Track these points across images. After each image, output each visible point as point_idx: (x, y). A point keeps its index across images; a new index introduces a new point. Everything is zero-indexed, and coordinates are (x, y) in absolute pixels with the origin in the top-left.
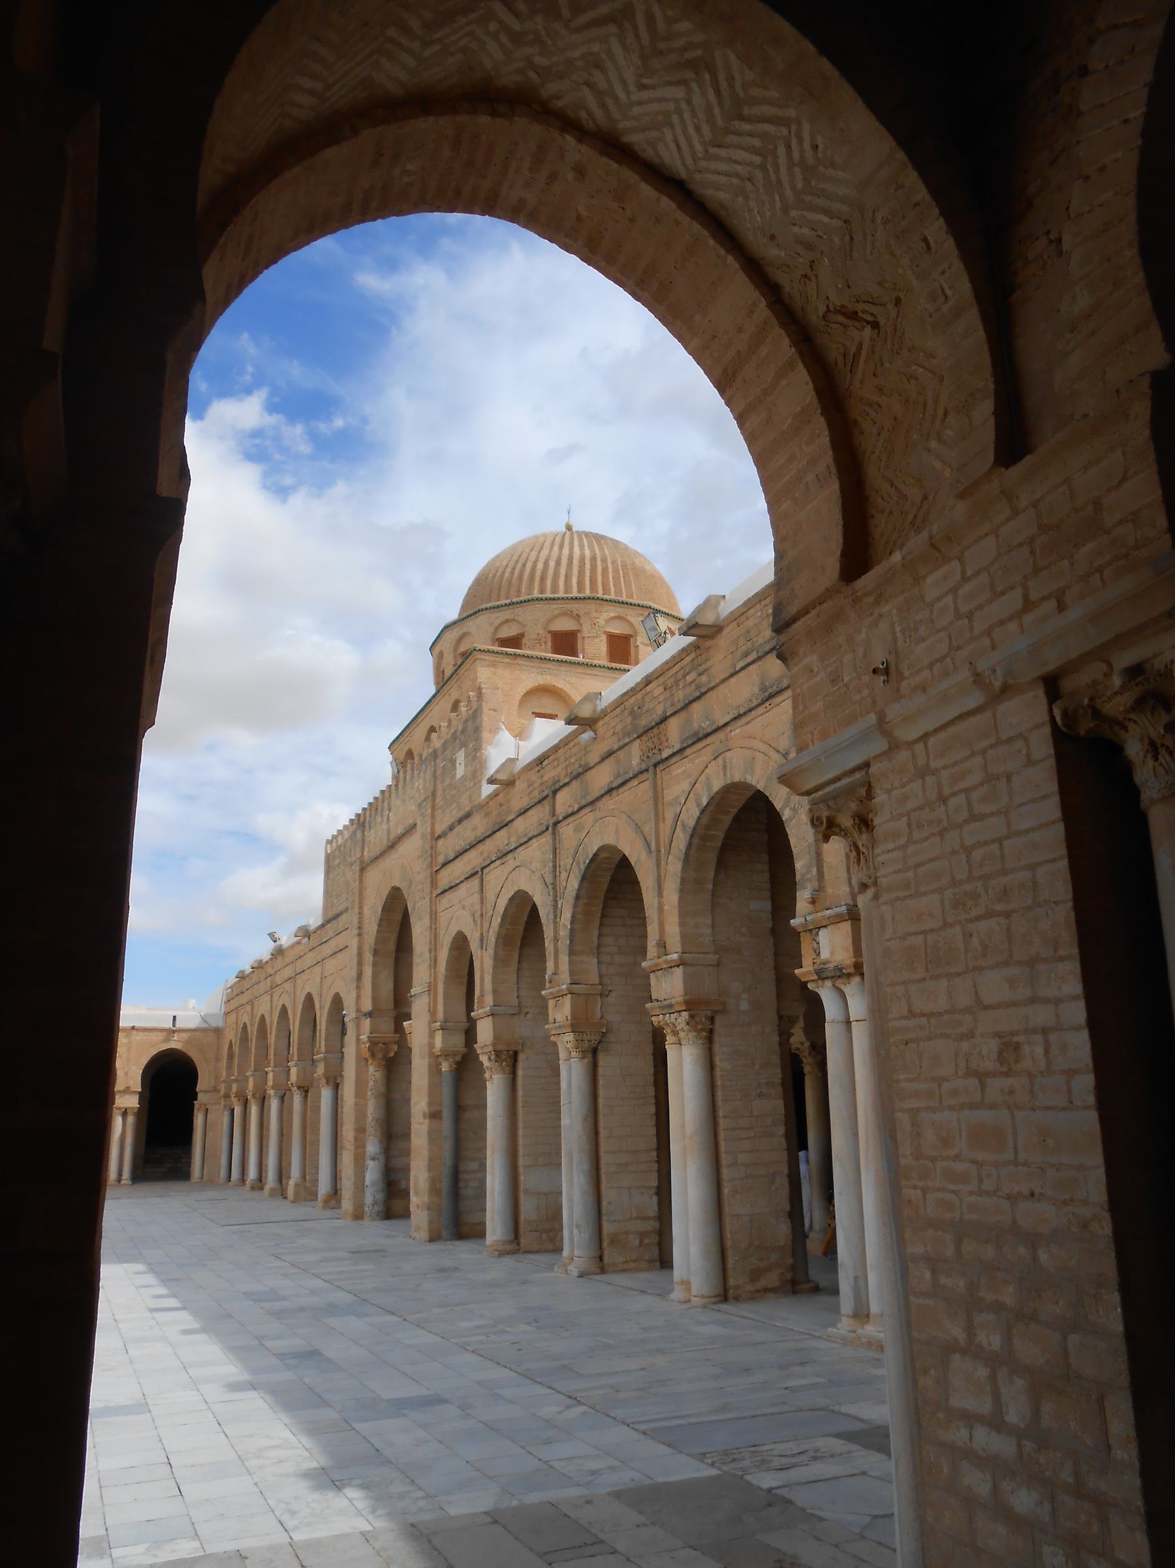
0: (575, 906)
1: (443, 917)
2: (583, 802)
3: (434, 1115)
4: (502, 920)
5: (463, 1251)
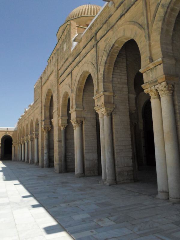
0: (105, 66)
1: (61, 90)
2: (109, 28)
3: (60, 141)
4: (78, 83)
5: (68, 177)
